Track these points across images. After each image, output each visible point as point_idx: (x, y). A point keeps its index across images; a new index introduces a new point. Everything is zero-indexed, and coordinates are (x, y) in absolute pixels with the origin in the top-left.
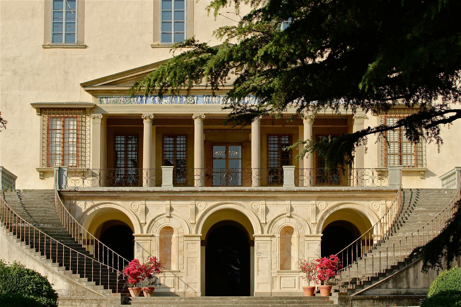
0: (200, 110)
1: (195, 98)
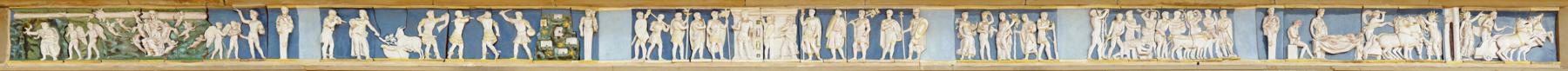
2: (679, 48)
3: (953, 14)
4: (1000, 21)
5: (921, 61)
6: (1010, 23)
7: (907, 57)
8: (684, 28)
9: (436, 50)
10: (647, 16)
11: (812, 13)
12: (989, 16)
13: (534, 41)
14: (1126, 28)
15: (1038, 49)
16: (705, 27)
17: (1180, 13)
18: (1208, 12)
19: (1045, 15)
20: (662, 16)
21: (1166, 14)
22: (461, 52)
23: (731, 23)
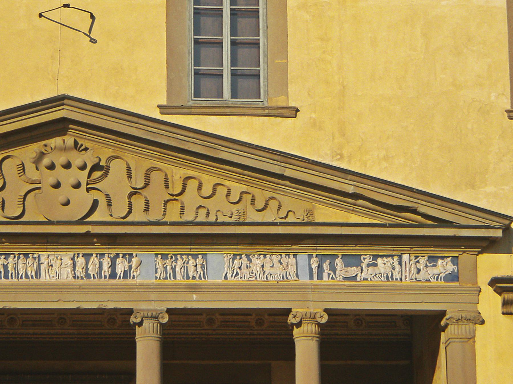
3: (154, 255)
4: (178, 259)
5: (137, 281)
6: (183, 260)
8: (14, 263)
11: (81, 255)
12: (172, 257)
14: (242, 263)
16: (26, 262)
17: (269, 256)
18: (284, 255)
19: (200, 257)
21: (262, 256)
23: (39, 260)
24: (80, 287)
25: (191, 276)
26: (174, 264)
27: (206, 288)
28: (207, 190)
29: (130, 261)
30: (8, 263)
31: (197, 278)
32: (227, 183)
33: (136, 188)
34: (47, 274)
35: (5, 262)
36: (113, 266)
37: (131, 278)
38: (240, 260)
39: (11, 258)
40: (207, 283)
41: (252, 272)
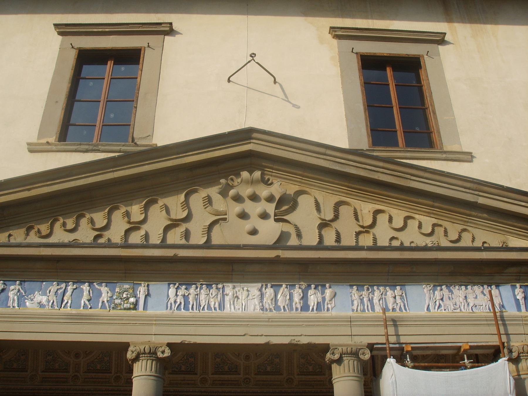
0: (154, 329)
1: (142, 291)
2: (193, 305)
6: (380, 292)
7: (324, 310)
8: (196, 293)
9: (55, 303)
10: (176, 286)
13: (111, 300)
14: (443, 295)
15: (397, 306)
20: (184, 287)
22: (69, 304)
24: (269, 319)
25: (390, 307)
26: (371, 295)
27: (407, 321)
28: (398, 223)
29: (323, 293)
30: (189, 294)
31: (398, 310)
32: (417, 216)
33: (325, 219)
34: (232, 307)
35: (186, 293)
36: (304, 298)
37: (326, 310)
38: (441, 291)
39: (193, 288)
40: (408, 314)
41: (456, 304)
